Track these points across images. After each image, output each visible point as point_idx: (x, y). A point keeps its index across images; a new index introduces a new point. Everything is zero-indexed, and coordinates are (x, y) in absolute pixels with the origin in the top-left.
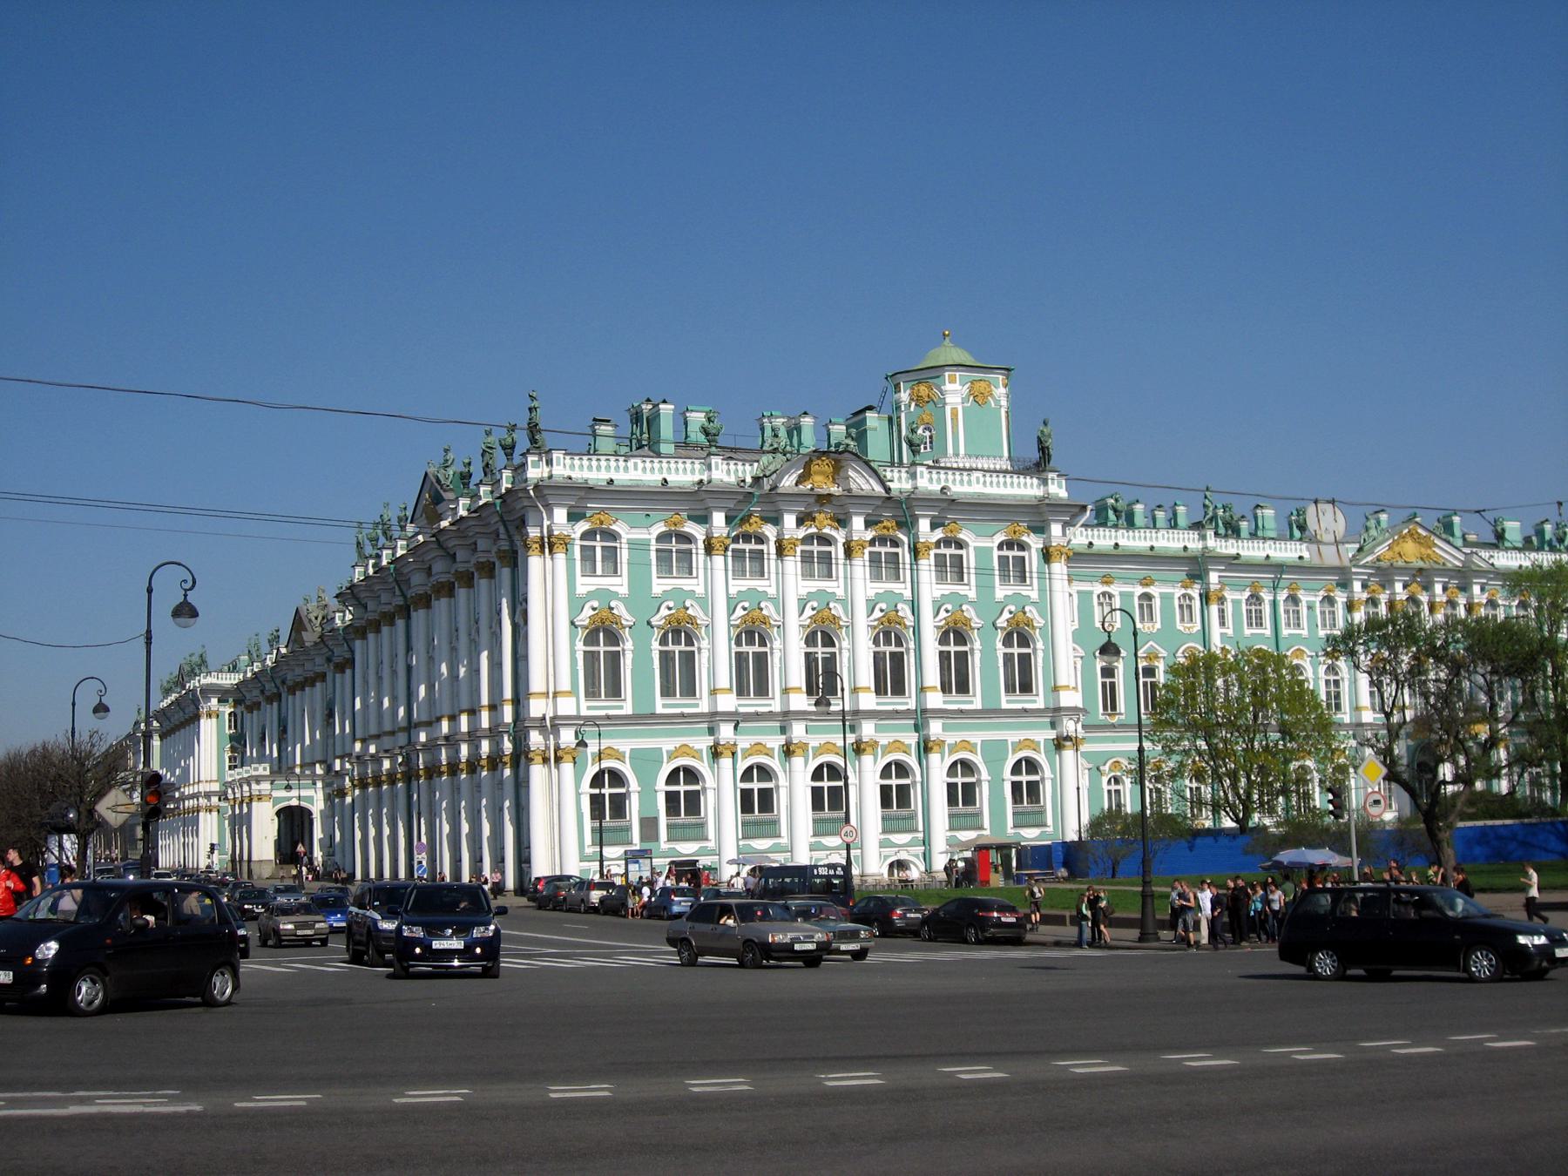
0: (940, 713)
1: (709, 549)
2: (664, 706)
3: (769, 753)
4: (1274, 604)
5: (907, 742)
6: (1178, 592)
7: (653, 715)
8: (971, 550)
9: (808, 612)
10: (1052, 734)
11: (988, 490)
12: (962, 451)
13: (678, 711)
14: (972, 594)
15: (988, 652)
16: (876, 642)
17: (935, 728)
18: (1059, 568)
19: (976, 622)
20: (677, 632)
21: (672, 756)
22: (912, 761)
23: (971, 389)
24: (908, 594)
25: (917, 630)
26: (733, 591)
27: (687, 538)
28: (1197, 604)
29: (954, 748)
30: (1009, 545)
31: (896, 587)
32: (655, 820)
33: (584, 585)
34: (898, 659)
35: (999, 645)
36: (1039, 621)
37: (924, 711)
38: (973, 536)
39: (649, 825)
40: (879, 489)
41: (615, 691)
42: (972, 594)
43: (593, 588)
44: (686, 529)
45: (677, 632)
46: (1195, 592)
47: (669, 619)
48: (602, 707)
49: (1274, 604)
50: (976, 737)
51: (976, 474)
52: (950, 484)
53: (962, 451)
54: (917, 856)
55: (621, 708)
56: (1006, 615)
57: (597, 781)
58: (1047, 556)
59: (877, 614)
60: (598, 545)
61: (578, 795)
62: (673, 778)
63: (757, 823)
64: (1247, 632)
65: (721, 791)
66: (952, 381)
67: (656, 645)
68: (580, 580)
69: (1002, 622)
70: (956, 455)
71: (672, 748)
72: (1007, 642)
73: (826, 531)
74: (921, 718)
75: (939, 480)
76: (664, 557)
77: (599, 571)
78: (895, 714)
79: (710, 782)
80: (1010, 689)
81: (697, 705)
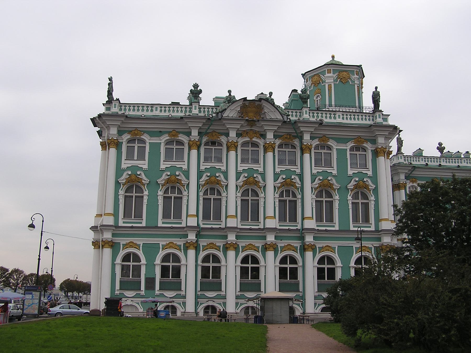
0: (311, 230)
3: (218, 248)
5: (295, 245)
7: (157, 227)
8: (335, 150)
9: (242, 179)
10: (377, 244)
11: (345, 121)
12: (333, 103)
14: (335, 172)
15: (343, 202)
16: (281, 195)
17: (309, 239)
19: (336, 186)
20: (173, 188)
21: (164, 248)
22: (297, 256)
24: (298, 171)
27: (180, 143)
29: (321, 249)
30: (358, 149)
31: (292, 168)
32: (153, 279)
33: (125, 164)
34: (293, 204)
35: (350, 198)
36: (372, 186)
37: (303, 229)
38: (336, 143)
39: (150, 283)
41: (139, 215)
42: (335, 172)
43: (130, 165)
44: (180, 138)
45: (173, 188)
47: (168, 181)
50: (335, 244)
51: (338, 114)
52: (324, 119)
53: (333, 103)
56: (353, 183)
58: (376, 153)
59: (280, 180)
60: (136, 146)
61: (113, 265)
62: (166, 258)
63: (211, 283)
65: (190, 265)
66: (329, 72)
67: (160, 193)
69: (351, 186)
70: (330, 105)
71: (164, 243)
72: (355, 196)
73: (253, 139)
74: (301, 234)
75: (318, 116)
76: (169, 152)
77: (136, 158)
79: (183, 261)
81: (181, 223)
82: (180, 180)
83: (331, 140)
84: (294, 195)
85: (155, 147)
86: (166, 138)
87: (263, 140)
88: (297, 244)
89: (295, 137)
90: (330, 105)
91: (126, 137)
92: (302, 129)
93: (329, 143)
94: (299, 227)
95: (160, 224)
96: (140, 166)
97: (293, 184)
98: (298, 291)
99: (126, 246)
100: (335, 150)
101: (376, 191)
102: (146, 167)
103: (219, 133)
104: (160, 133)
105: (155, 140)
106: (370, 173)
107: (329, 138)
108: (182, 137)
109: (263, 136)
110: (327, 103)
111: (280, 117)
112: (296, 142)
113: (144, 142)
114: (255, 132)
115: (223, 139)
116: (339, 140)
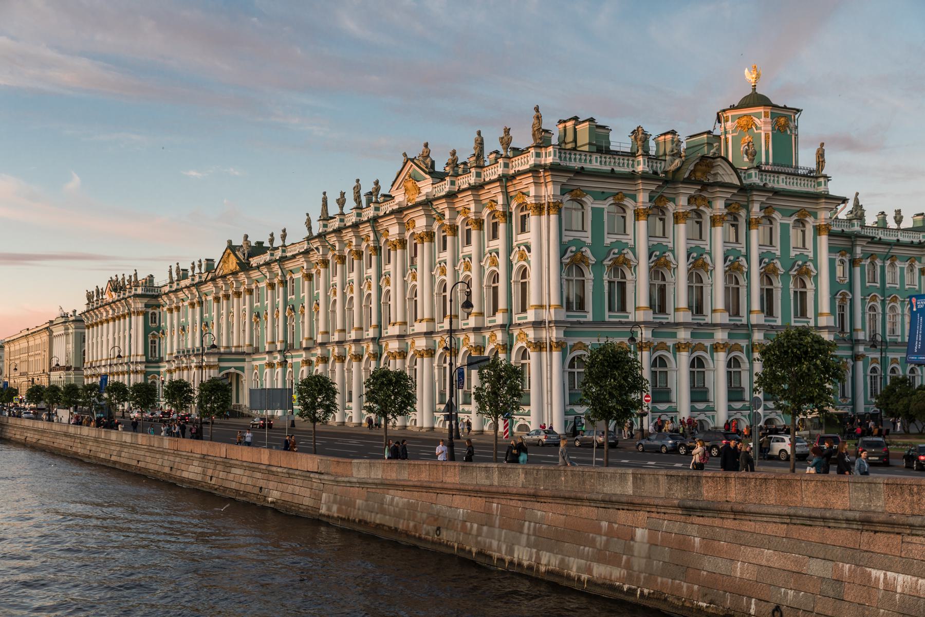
1: (637, 215)
2: (610, 317)
4: (883, 268)
6: (838, 258)
7: (604, 323)
12: (771, 161)
13: (617, 320)
14: (778, 253)
18: (824, 240)
19: (781, 271)
23: (777, 122)
24: (744, 251)
26: (651, 243)
28: (847, 264)
35: (791, 286)
40: (737, 182)
43: (571, 238)
45: (616, 270)
46: (846, 259)
48: (576, 316)
49: (883, 268)
53: (771, 161)
54: (745, 416)
55: (586, 317)
57: (572, 365)
64: (868, 284)
68: (564, 233)
70: (767, 163)
73: (701, 208)
78: (736, 326)
80: (796, 316)
82: (629, 260)
83: (776, 213)
84: (737, 283)
85: (597, 213)
86: (611, 201)
87: (710, 210)
88: (744, 343)
89: (743, 207)
90: (767, 163)
91: (567, 197)
92: (755, 198)
93: (774, 216)
94: (744, 321)
95: (607, 319)
96: (583, 239)
97: (739, 268)
98: (743, 400)
99: (573, 348)
100: (778, 225)
101: (816, 277)
102: (589, 241)
103: (667, 198)
104: (603, 196)
105: (599, 205)
106: (811, 255)
107: (774, 210)
108: (628, 202)
109: (709, 204)
110: (763, 160)
111: (737, 182)
112: (743, 213)
113: (582, 204)
114: (704, 199)
115: (671, 207)
116: (787, 213)
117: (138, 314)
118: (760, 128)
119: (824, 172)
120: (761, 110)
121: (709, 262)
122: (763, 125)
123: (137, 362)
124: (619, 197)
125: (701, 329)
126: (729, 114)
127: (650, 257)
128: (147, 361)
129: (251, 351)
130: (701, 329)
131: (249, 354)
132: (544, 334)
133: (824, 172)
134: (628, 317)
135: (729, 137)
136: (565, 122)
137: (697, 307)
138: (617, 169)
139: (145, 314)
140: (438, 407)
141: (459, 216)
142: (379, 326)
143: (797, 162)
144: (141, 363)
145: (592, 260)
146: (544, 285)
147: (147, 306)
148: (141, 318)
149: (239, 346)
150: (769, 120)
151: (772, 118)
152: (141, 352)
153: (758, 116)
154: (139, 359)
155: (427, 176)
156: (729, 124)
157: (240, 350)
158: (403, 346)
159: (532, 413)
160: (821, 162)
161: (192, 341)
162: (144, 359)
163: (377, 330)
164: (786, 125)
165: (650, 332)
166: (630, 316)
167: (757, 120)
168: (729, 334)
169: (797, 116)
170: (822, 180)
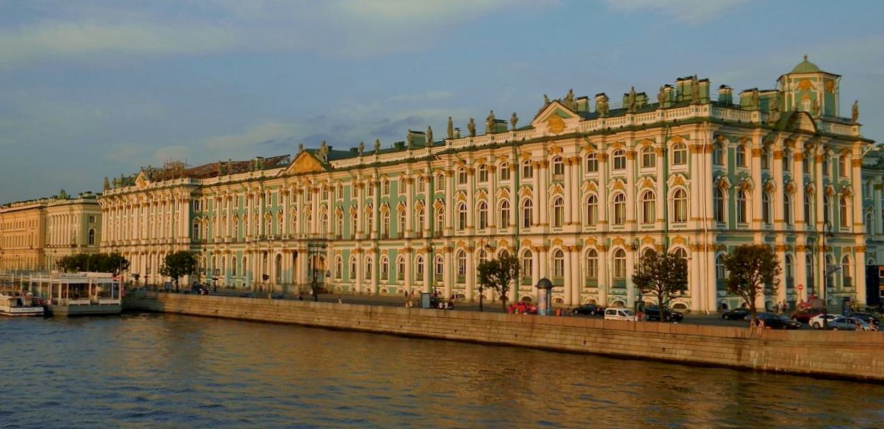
2: (738, 226)
7: (736, 231)
25: (816, 195)
40: (813, 130)
55: (724, 226)
111: (813, 130)
117: (185, 201)
118: (816, 89)
119: (857, 121)
120: (817, 76)
121: (814, 188)
122: (818, 87)
123: (183, 244)
124: (744, 140)
125: (791, 234)
126: (792, 77)
127: (714, 180)
128: (192, 243)
129: (332, 239)
130: (791, 234)
131: (331, 241)
132: (701, 239)
133: (857, 121)
134: (747, 226)
135: (793, 94)
136: (682, 80)
137: (787, 218)
138: (742, 120)
139: (191, 203)
140: (476, 285)
141: (610, 148)
142: (517, 225)
143: (839, 113)
144: (187, 244)
145: (730, 185)
146: (700, 203)
147: (192, 194)
148: (187, 205)
149: (316, 234)
150: (822, 83)
151: (824, 82)
152: (186, 234)
153: (815, 79)
154: (185, 241)
155: (576, 115)
156: (792, 84)
157: (317, 237)
158: (547, 242)
159: (466, 288)
160: (855, 114)
161: (252, 227)
162: (189, 241)
163: (516, 229)
164: (832, 87)
165: (785, 238)
166: (750, 226)
167: (812, 82)
168: (766, 238)
169: (838, 80)
170: (856, 127)
